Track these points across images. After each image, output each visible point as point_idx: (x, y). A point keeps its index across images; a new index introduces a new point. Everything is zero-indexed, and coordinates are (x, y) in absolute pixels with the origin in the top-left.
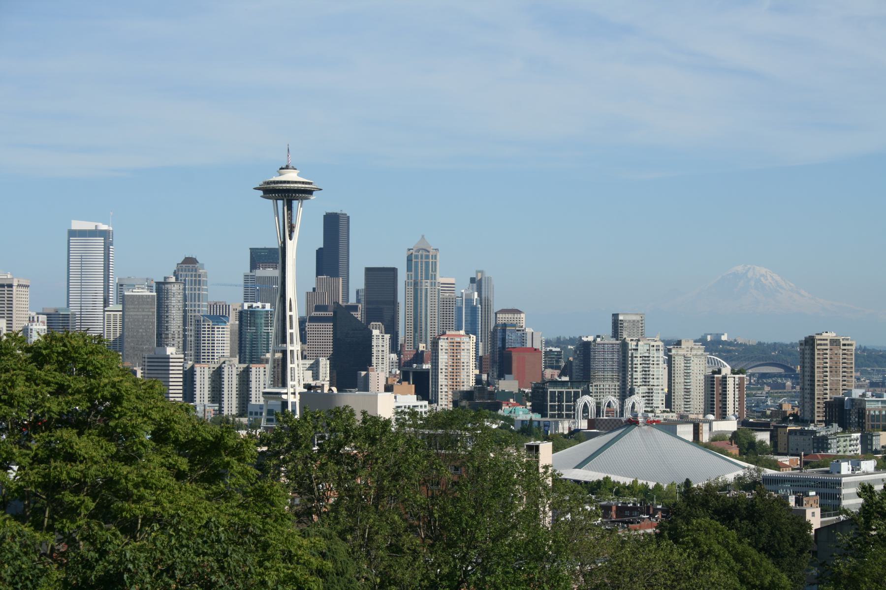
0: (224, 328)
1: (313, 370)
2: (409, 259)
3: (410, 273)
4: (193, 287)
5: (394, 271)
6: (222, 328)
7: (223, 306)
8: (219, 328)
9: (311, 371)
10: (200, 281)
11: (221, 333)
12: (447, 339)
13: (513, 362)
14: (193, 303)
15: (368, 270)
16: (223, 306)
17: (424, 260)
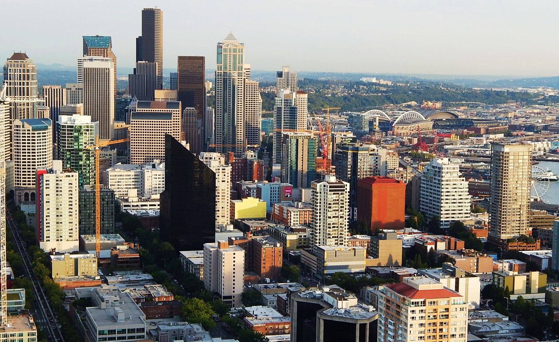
0: (45, 133)
1: (137, 188)
2: (219, 54)
3: (220, 65)
4: (22, 81)
5: (202, 58)
6: (43, 133)
7: (57, 89)
8: (40, 133)
9: (136, 190)
10: (28, 76)
11: (41, 138)
12: (424, 303)
13: (373, 197)
15: (180, 58)
16: (57, 89)
17: (232, 53)
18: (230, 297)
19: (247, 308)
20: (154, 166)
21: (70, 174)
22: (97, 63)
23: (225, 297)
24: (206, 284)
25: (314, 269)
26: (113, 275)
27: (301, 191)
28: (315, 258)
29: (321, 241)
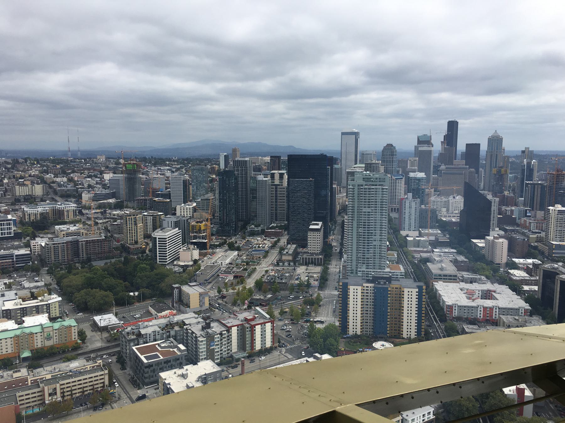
4: (390, 157)
5: (478, 145)
10: (393, 154)
14: (390, 164)
15: (467, 144)
18: (499, 264)
19: (509, 271)
20: (454, 197)
21: (416, 200)
22: (425, 148)
23: (496, 264)
24: (486, 256)
25: (547, 254)
26: (436, 248)
27: (536, 212)
28: (547, 248)
29: (551, 239)
